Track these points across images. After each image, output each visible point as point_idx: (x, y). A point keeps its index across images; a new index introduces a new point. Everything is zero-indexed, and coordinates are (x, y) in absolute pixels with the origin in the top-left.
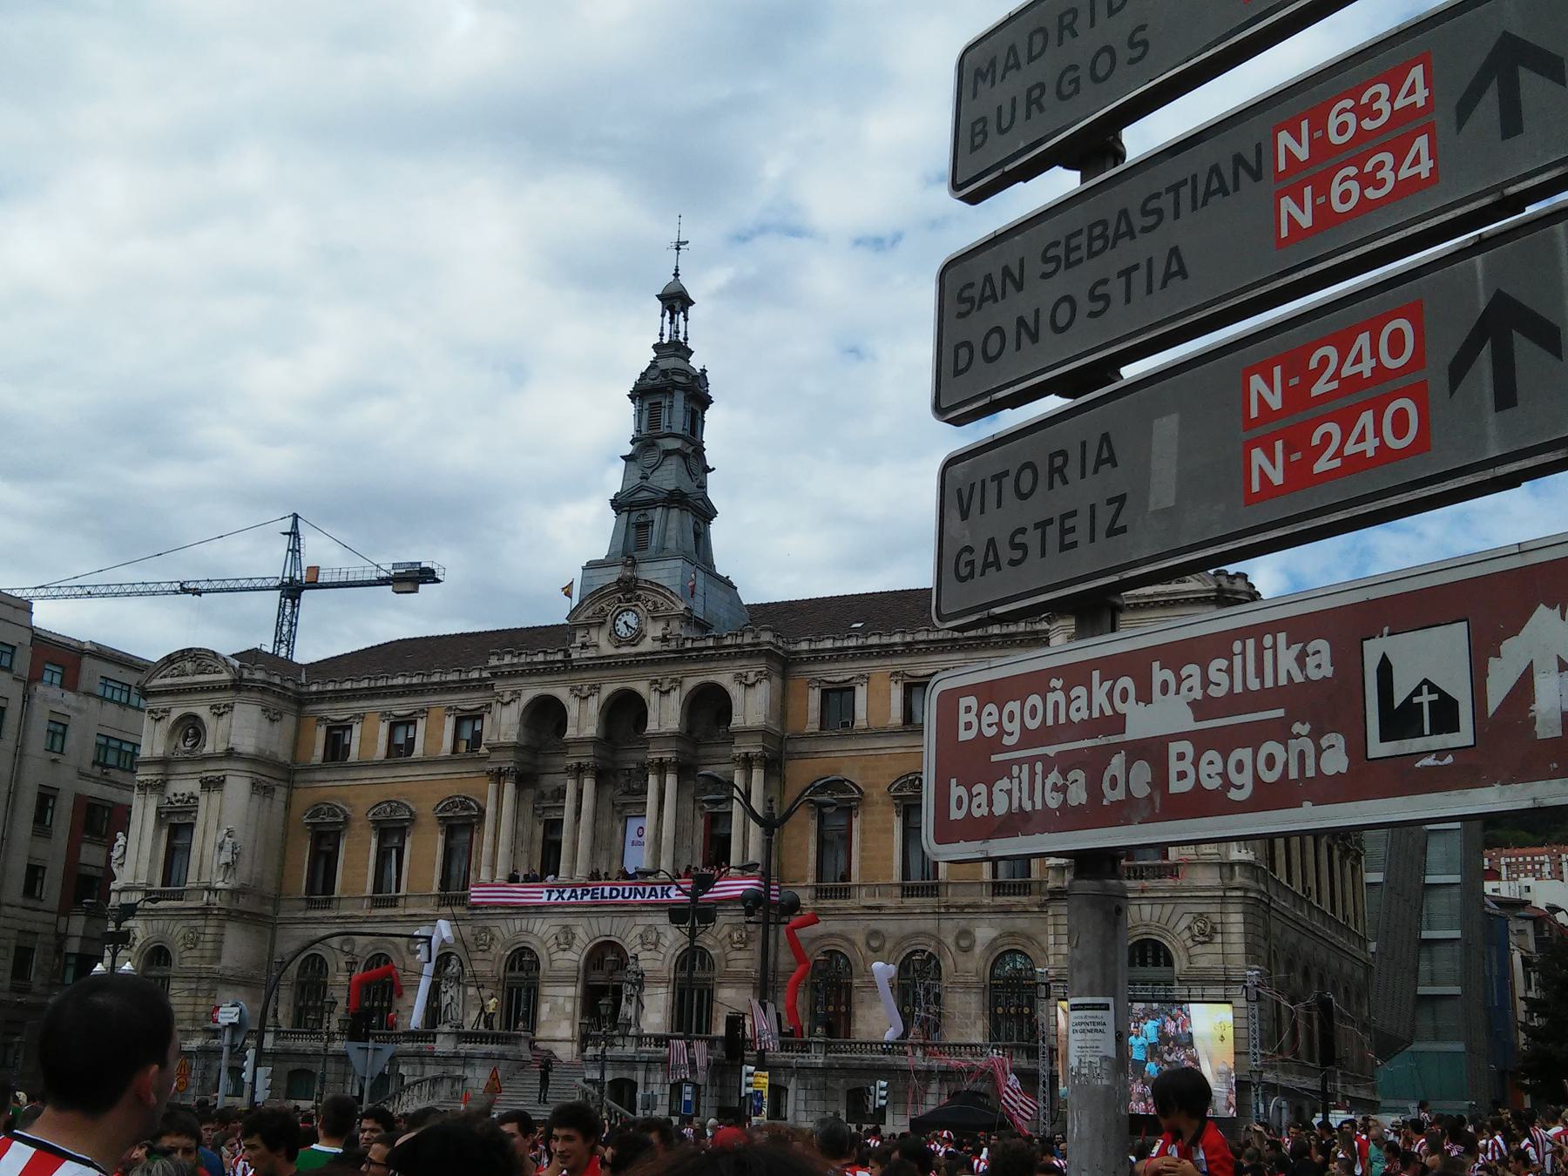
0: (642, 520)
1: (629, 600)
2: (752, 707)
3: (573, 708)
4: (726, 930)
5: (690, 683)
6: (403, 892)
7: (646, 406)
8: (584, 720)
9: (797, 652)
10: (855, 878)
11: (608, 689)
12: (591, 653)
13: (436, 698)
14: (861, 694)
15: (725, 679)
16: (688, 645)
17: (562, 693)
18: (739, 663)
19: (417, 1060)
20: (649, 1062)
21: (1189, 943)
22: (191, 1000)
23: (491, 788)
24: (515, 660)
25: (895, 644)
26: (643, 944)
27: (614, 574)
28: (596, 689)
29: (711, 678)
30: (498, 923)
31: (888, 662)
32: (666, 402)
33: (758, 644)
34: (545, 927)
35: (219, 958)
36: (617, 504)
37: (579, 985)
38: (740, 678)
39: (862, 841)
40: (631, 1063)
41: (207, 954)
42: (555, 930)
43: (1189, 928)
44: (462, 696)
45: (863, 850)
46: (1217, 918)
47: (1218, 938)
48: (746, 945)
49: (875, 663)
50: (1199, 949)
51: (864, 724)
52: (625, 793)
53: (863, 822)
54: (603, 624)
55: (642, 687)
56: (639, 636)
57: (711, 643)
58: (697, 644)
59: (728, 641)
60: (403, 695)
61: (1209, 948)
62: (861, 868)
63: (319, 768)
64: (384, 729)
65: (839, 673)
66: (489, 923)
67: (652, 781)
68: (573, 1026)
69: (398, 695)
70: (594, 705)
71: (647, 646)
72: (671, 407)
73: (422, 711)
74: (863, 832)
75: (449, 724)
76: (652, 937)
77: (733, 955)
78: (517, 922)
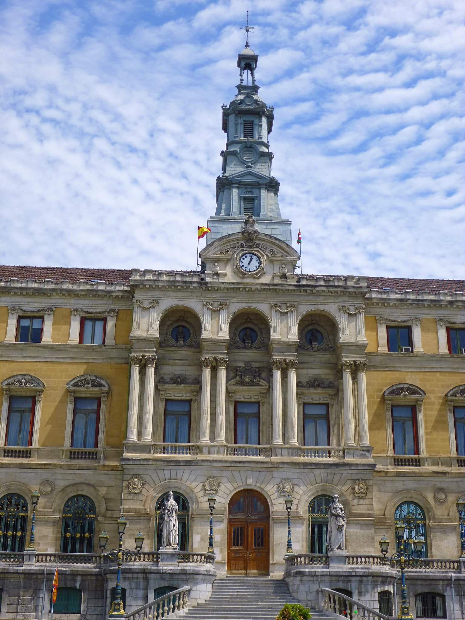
0: (249, 195)
1: (250, 247)
2: (352, 331)
5: (304, 309)
6: (36, 445)
7: (241, 121)
9: (371, 299)
10: (424, 453)
11: (235, 307)
12: (221, 280)
13: (61, 301)
14: (417, 333)
15: (331, 308)
16: (304, 282)
17: (195, 305)
18: (341, 300)
19: (141, 576)
20: (361, 576)
23: (136, 370)
24: (155, 278)
25: (441, 301)
27: (237, 228)
28: (225, 305)
29: (321, 307)
30: (150, 472)
31: (433, 311)
32: (256, 121)
33: (361, 287)
36: (224, 185)
37: (226, 521)
38: (343, 309)
40: (347, 577)
44: (87, 302)
48: (366, 494)
49: (424, 312)
51: (422, 350)
52: (238, 384)
53: (425, 415)
54: (228, 261)
55: (264, 308)
56: (260, 272)
57: (322, 283)
58: (309, 283)
59: (336, 284)
60: (33, 294)
62: (427, 447)
65: (401, 316)
66: (140, 472)
67: (277, 375)
68: (221, 551)
69: (27, 295)
70: (225, 319)
71: (266, 279)
72: (260, 126)
73: (50, 309)
76: (288, 488)
77: (355, 502)
78: (167, 474)
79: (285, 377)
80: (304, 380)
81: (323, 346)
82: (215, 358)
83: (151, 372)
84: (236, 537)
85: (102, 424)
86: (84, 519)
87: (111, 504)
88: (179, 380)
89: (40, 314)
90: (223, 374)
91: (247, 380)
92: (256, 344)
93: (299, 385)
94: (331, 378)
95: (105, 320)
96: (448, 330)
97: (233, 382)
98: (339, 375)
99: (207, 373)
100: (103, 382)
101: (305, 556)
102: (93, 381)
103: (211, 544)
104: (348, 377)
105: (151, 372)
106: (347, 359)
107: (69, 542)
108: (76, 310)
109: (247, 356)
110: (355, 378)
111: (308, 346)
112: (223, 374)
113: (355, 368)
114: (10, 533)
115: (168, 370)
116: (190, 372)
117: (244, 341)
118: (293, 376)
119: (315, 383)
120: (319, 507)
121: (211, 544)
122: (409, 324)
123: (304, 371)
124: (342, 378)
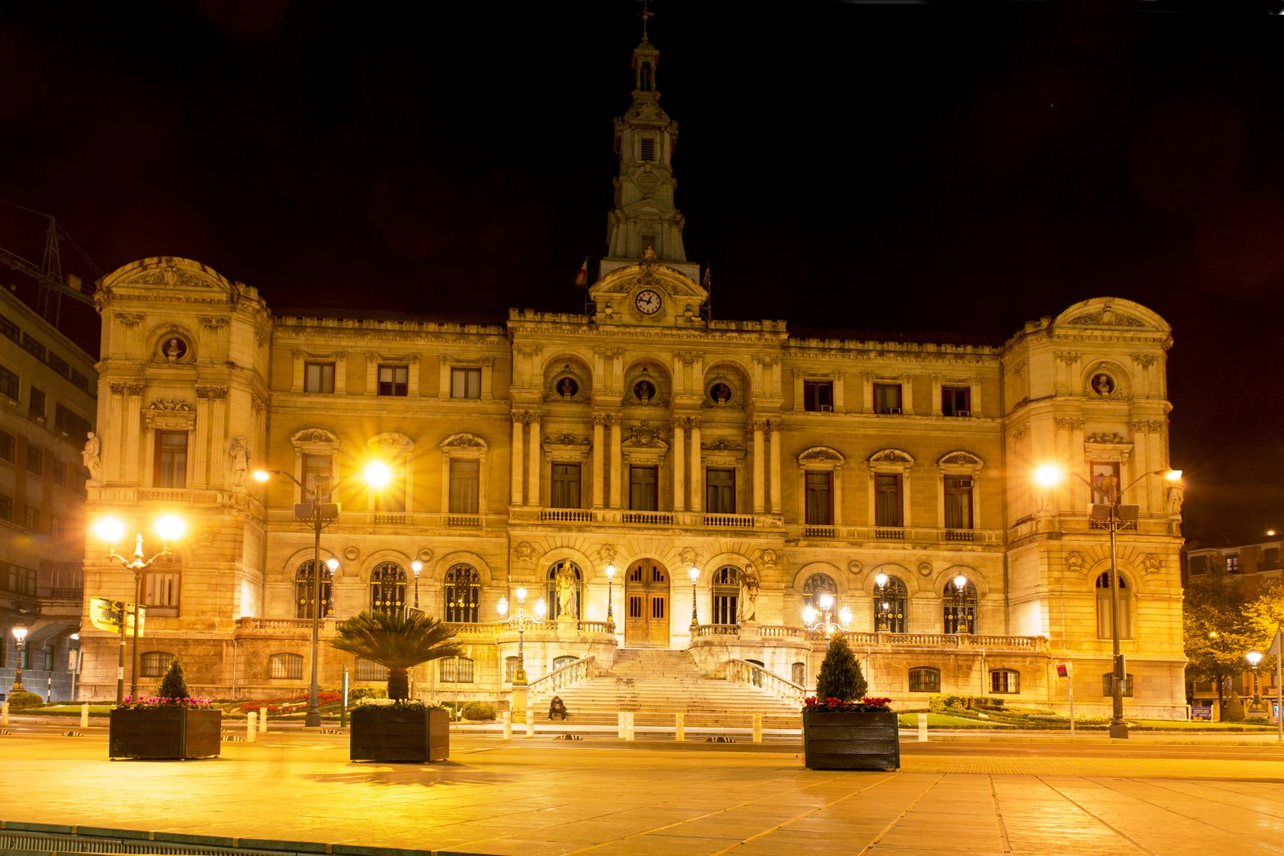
3: (599, 369)
4: (757, 554)
8: (609, 378)
15: (742, 358)
21: (1143, 573)
22: (211, 594)
23: (518, 427)
26: (683, 561)
29: (731, 357)
34: (586, 546)
35: (241, 556)
37: (623, 590)
39: (843, 496)
41: (228, 552)
42: (599, 547)
43: (1143, 562)
45: (843, 502)
46: (1162, 557)
47: (1163, 570)
50: (1150, 577)
53: (843, 482)
61: (1156, 576)
63: (297, 394)
64: (372, 369)
67: (679, 434)
70: (618, 367)
74: (843, 489)
75: (445, 372)
79: (688, 437)
80: (708, 442)
81: (730, 403)
82: (608, 416)
83: (535, 429)
84: (634, 608)
85: (482, 488)
86: (468, 589)
87: (496, 573)
88: (567, 440)
89: (404, 363)
90: (616, 432)
91: (644, 441)
92: (655, 399)
93: (704, 447)
94: (739, 439)
95: (479, 370)
96: (875, 386)
97: (628, 442)
98: (748, 434)
99: (599, 432)
100: (481, 441)
101: (709, 627)
102: (470, 441)
103: (610, 614)
104: (758, 437)
105: (535, 429)
106: (760, 418)
107: (453, 612)
108: (445, 359)
109: (645, 413)
110: (767, 440)
111: (713, 403)
112: (616, 432)
113: (768, 428)
114: (388, 603)
115: (553, 428)
116: (579, 430)
117: (639, 397)
118: (696, 435)
119: (720, 445)
120: (724, 577)
121: (610, 614)
122: (831, 378)
123: (708, 432)
124: (752, 440)
